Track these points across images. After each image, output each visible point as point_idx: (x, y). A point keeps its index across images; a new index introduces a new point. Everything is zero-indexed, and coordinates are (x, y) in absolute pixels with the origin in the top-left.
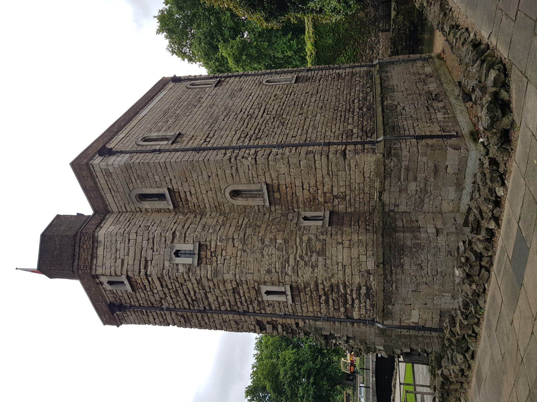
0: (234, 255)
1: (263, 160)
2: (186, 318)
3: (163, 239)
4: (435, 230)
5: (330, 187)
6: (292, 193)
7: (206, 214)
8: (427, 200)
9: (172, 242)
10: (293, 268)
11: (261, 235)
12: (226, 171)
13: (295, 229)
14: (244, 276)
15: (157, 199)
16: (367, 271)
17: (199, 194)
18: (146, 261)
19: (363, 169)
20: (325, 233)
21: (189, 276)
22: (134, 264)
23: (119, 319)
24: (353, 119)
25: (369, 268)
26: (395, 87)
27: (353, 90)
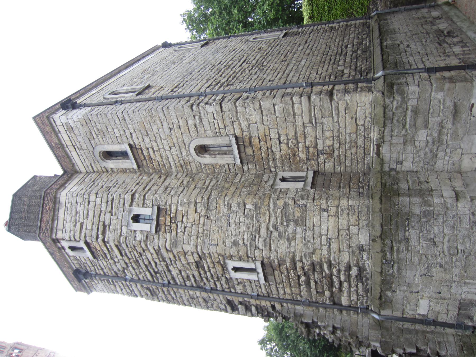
0: (196, 222)
1: (230, 106)
2: (152, 291)
3: (122, 201)
4: (454, 193)
5: (313, 139)
6: (267, 147)
7: (171, 175)
8: (441, 155)
9: (131, 205)
10: (265, 241)
11: (228, 199)
12: (189, 122)
13: (269, 192)
14: (206, 248)
15: (122, 158)
16: (359, 247)
17: (162, 150)
18: (104, 226)
20: (305, 197)
21: (146, 245)
22: (92, 229)
24: (345, 62)
25: (363, 242)
26: (397, 30)
27: (347, 38)
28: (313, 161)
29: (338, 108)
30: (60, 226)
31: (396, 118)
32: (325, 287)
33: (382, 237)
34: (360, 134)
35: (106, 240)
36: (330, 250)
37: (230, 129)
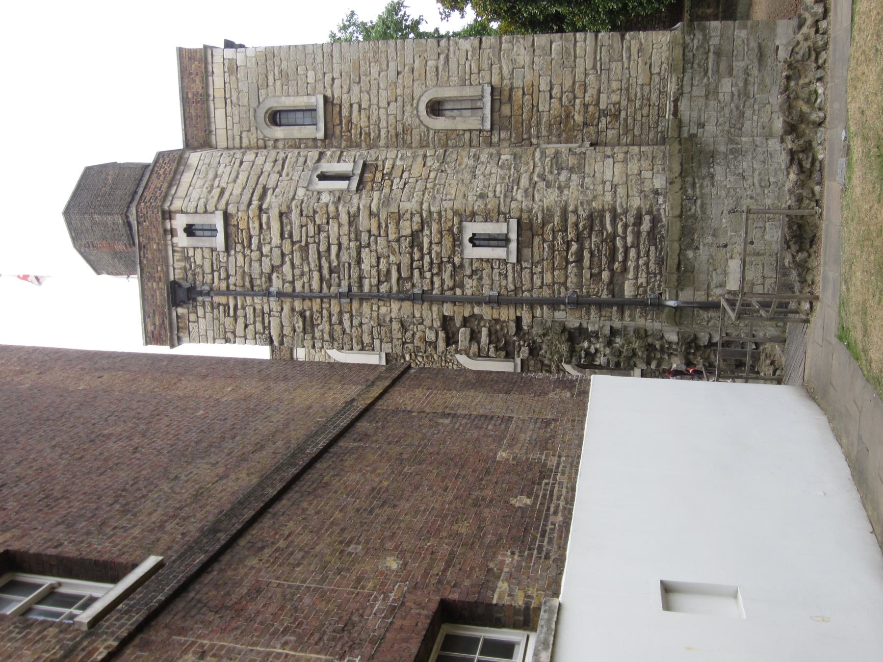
0: (423, 177)
2: (308, 319)
3: (302, 159)
5: (596, 92)
6: (532, 104)
8: (748, 113)
9: (319, 160)
10: (526, 191)
12: (430, 63)
14: (437, 203)
17: (374, 107)
18: (265, 190)
19: (650, 58)
21: (337, 208)
22: (241, 194)
23: (178, 328)
28: (591, 127)
29: (629, 49)
30: (182, 191)
31: (697, 62)
32: (604, 260)
33: (682, 174)
34: (654, 87)
35: (264, 207)
36: (616, 196)
37: (485, 74)
